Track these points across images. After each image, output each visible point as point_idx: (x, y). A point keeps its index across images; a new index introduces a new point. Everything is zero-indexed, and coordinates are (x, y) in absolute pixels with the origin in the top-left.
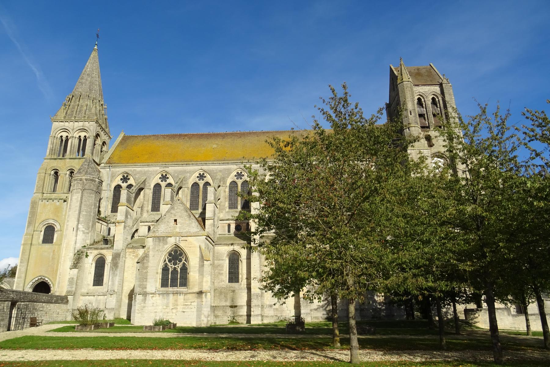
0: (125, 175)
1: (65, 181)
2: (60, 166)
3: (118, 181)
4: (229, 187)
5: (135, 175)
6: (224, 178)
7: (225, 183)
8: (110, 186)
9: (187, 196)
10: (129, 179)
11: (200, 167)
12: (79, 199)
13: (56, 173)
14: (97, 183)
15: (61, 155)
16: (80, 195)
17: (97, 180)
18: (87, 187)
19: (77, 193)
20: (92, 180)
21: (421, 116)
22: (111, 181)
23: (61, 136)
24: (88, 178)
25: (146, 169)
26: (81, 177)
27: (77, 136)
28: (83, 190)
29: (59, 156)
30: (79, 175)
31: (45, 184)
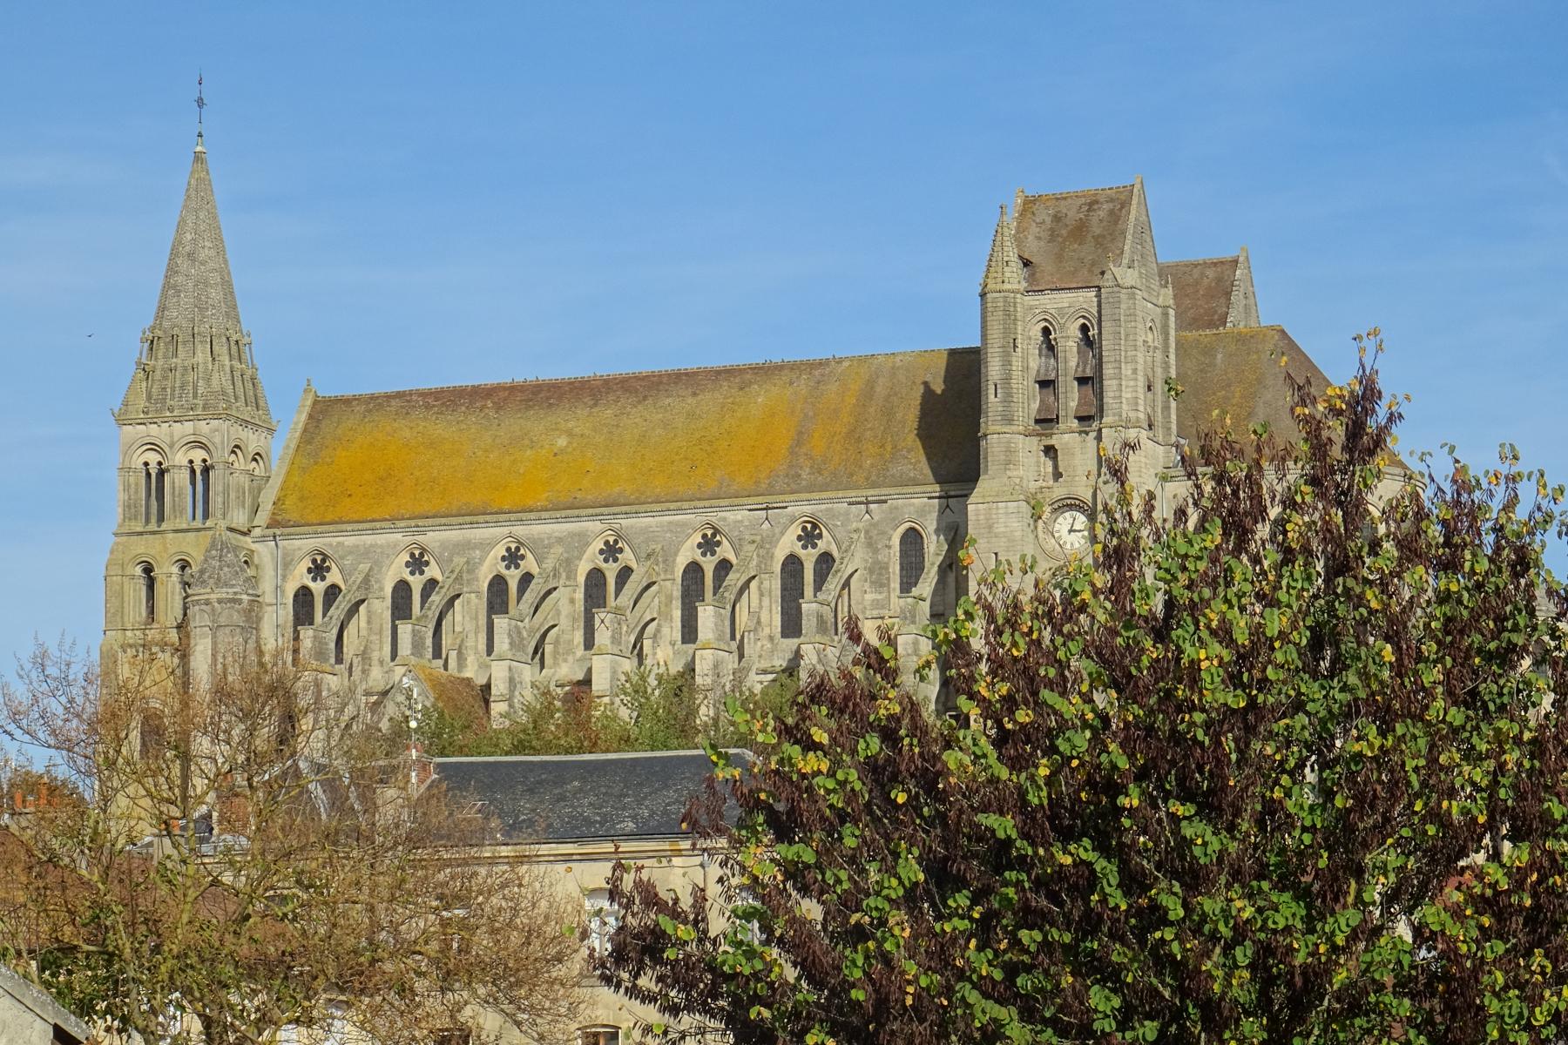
0: (319, 558)
1: (173, 593)
2: (153, 552)
3: (300, 576)
4: (586, 585)
5: (342, 558)
6: (568, 562)
7: (571, 575)
8: (283, 592)
9: (476, 618)
10: (328, 569)
11: (506, 530)
12: (210, 652)
13: (148, 570)
14: (245, 604)
15: (154, 519)
16: (209, 641)
17: (245, 597)
18: (223, 620)
19: (203, 636)
20: (234, 601)
21: (1045, 384)
22: (284, 577)
23: (146, 464)
24: (224, 596)
25: (369, 539)
26: (206, 597)
27: (185, 462)
28: (215, 629)
29: (148, 521)
30: (202, 591)
31: (126, 605)
